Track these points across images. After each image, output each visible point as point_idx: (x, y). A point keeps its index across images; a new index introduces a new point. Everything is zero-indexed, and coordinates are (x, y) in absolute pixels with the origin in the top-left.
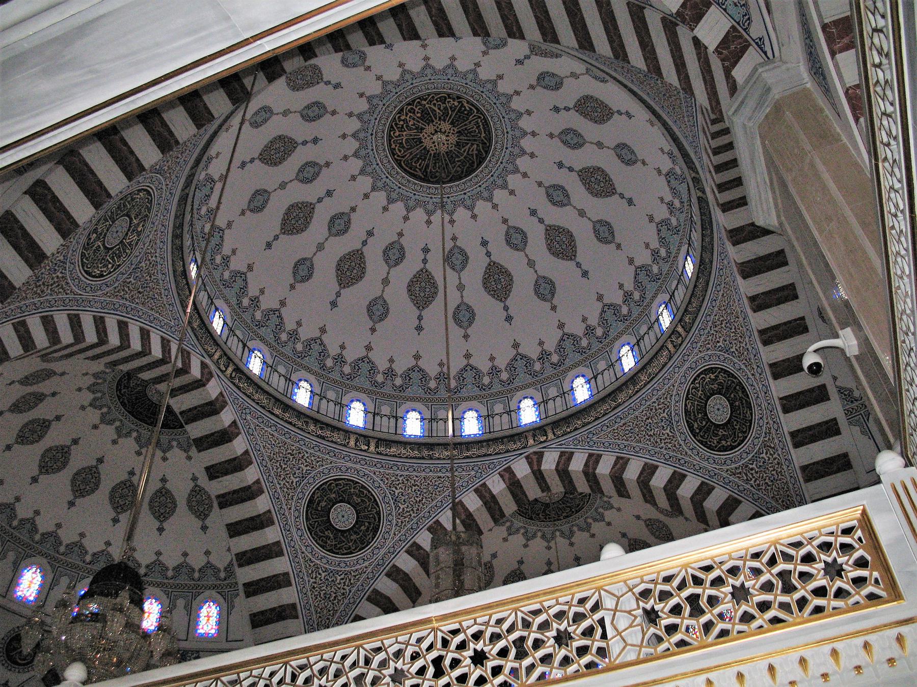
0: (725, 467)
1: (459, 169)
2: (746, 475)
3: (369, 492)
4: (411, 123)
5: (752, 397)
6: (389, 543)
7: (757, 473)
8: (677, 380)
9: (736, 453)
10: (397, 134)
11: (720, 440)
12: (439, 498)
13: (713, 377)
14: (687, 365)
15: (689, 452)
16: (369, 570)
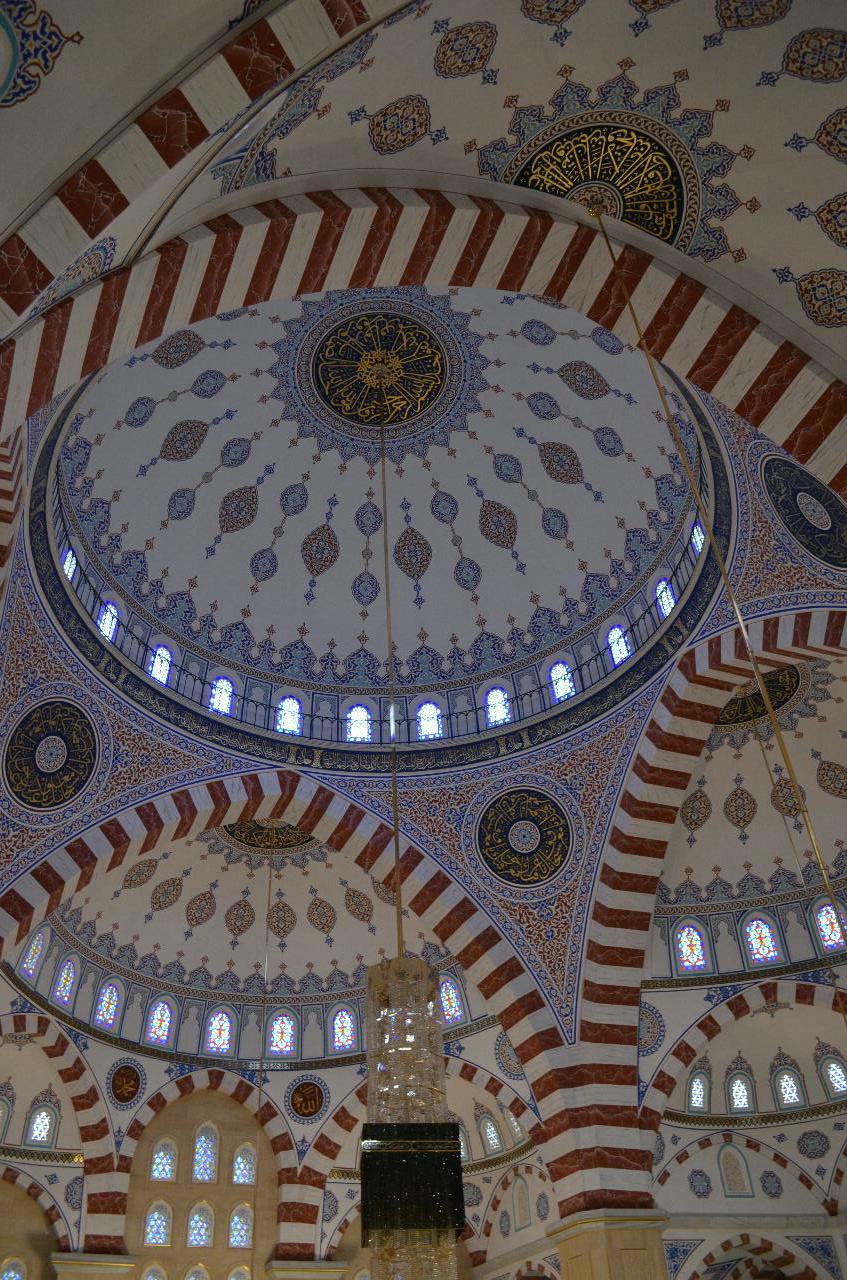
0: (500, 896)
1: (368, 412)
2: (521, 916)
3: (92, 733)
4: (369, 335)
5: (573, 847)
6: (88, 809)
7: (534, 919)
8: (490, 781)
10: (345, 334)
11: (509, 867)
12: (165, 777)
13: (537, 802)
14: (512, 774)
15: (467, 861)
16: (51, 835)
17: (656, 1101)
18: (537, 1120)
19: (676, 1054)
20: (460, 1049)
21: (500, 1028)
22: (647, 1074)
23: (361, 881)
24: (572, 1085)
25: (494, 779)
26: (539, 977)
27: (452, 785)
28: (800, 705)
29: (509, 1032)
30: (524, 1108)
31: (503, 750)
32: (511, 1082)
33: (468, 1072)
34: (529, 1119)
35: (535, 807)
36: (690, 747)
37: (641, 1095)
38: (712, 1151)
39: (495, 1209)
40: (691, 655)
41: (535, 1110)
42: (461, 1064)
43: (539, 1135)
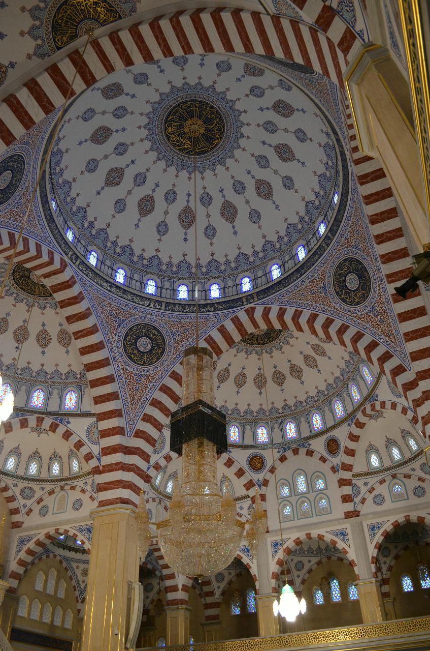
0: (123, 364)
1: (174, 139)
4: (204, 112)
8: (142, 315)
9: (133, 365)
10: (197, 105)
11: (132, 353)
17: (152, 472)
18: (97, 464)
19: (165, 458)
20: (68, 422)
21: (95, 419)
22: (152, 461)
23: (54, 331)
24: (125, 453)
25: (142, 315)
26: (125, 404)
27: (124, 308)
28: (268, 349)
29: (99, 423)
30: (93, 457)
31: (152, 305)
32: (90, 445)
33: (67, 435)
34: (93, 463)
35: (154, 335)
36: (230, 341)
37: (149, 468)
38: (155, 504)
39: (38, 503)
40: (254, 309)
41: (99, 460)
42: (65, 429)
43: (97, 471)
